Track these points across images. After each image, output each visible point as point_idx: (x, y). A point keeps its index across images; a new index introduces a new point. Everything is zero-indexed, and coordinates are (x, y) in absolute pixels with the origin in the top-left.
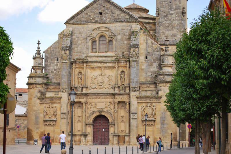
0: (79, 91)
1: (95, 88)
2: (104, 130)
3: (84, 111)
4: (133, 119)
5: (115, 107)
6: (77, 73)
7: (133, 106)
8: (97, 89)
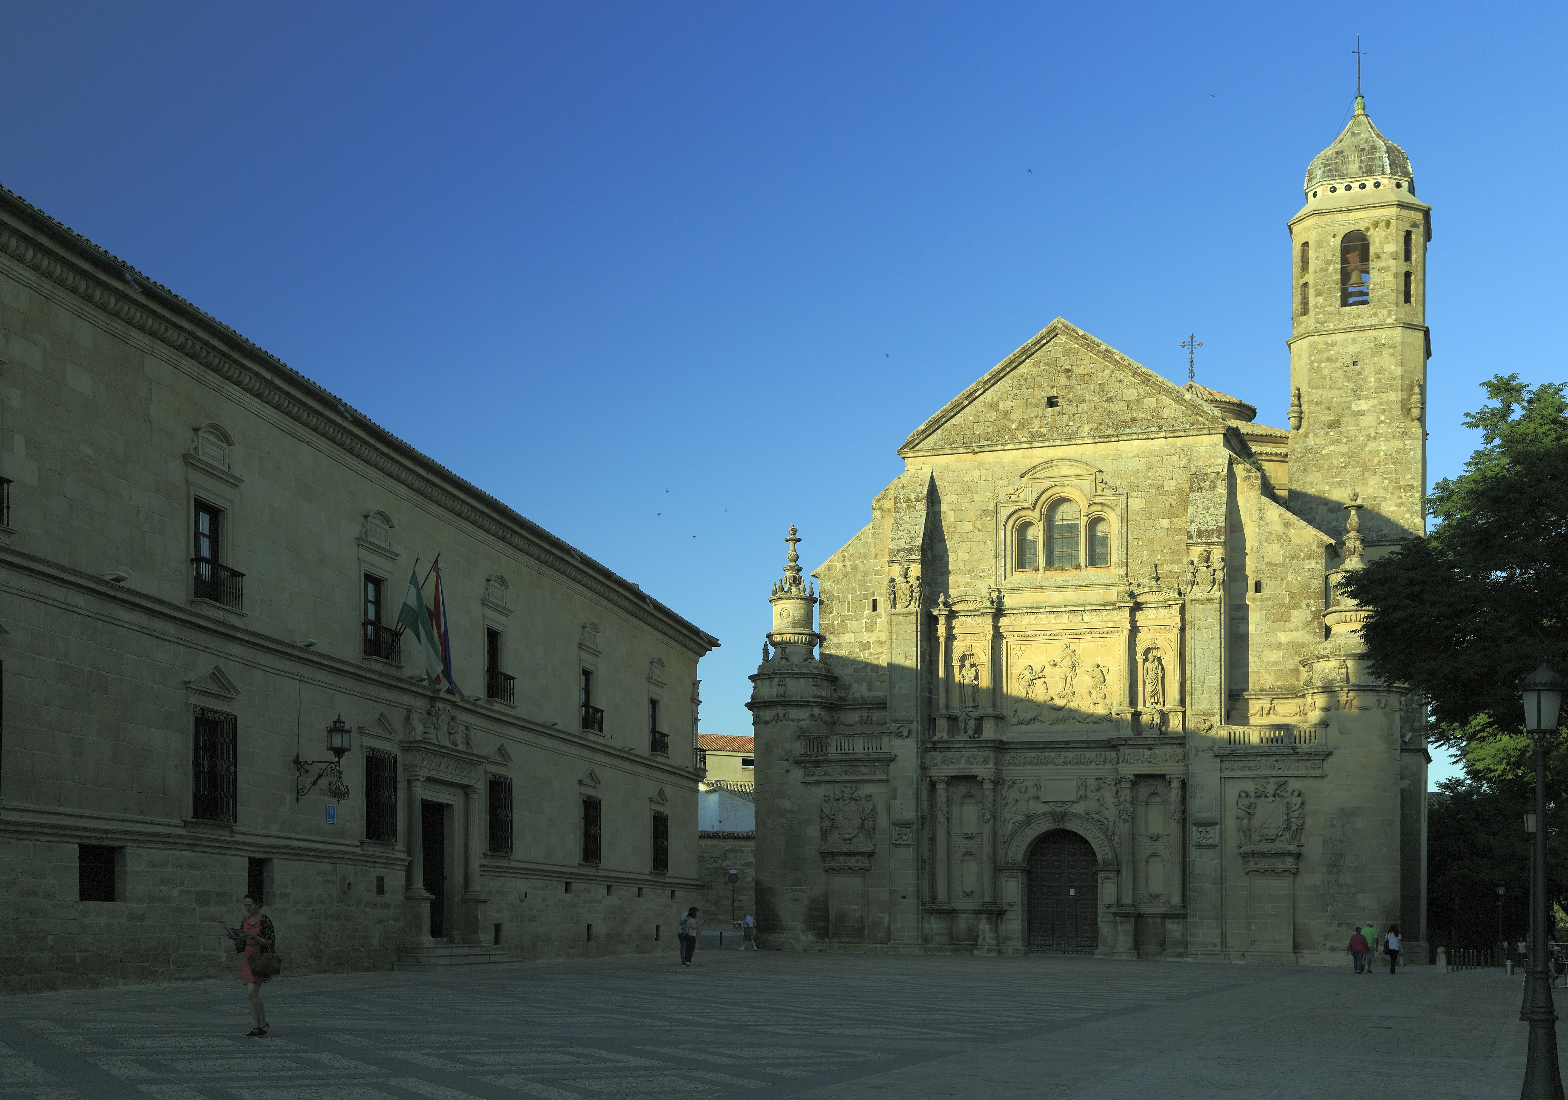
0: (966, 732)
3: (987, 814)
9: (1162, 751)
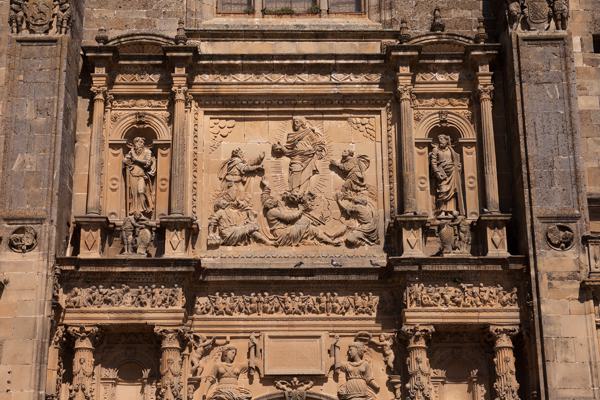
0: (135, 250)
1: (248, 238)
5: (413, 367)
6: (116, 134)
7: (560, 357)
8: (259, 241)
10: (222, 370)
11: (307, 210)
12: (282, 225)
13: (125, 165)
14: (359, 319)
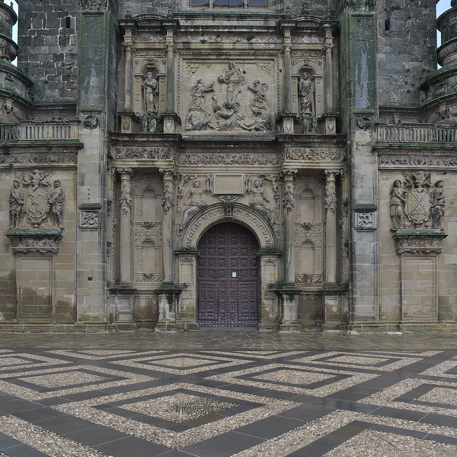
1: (205, 126)
2: (238, 275)
4: (361, 229)
5: (287, 190)
8: (212, 128)
9: (319, 149)
10: (193, 191)
11: (235, 112)
12: (223, 120)
13: (142, 86)
14: (261, 167)
